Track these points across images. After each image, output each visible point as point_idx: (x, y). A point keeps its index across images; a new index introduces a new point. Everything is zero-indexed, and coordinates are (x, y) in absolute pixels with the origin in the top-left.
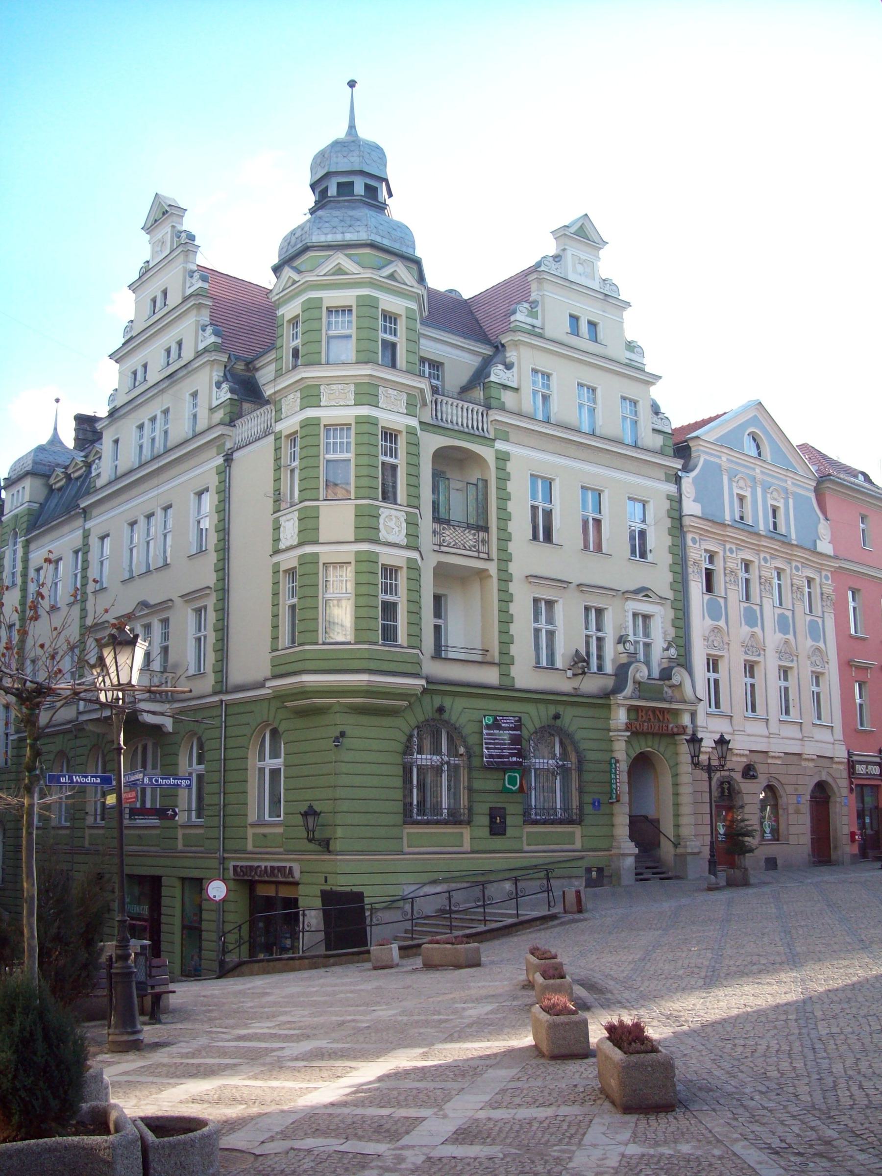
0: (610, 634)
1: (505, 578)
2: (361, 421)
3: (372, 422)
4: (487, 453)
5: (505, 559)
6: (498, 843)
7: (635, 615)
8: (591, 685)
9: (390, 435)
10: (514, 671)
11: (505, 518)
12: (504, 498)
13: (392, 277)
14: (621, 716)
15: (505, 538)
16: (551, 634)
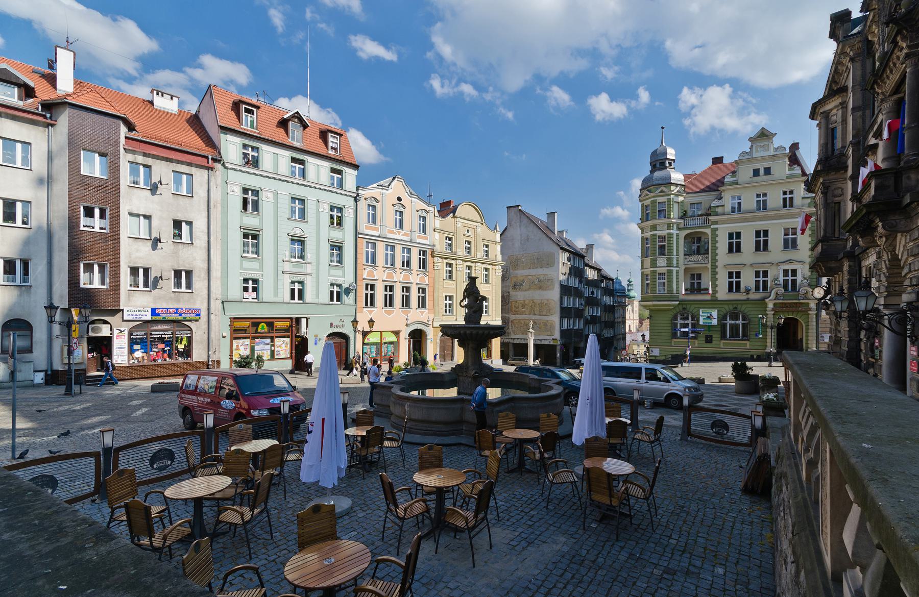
0: (769, 279)
1: (714, 267)
2: (652, 235)
3: (655, 235)
4: (708, 231)
5: (714, 261)
6: (708, 345)
7: (786, 272)
8: (754, 296)
9: (662, 238)
10: (717, 295)
11: (715, 248)
12: (715, 242)
13: (662, 191)
14: (770, 306)
15: (715, 255)
16: (738, 283)
